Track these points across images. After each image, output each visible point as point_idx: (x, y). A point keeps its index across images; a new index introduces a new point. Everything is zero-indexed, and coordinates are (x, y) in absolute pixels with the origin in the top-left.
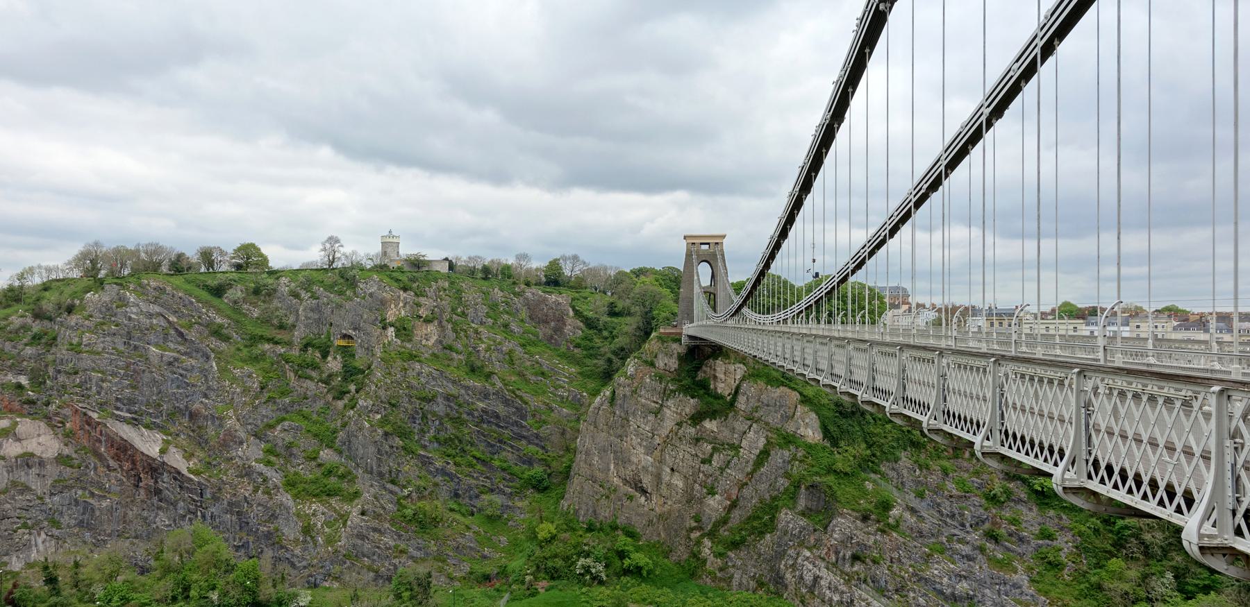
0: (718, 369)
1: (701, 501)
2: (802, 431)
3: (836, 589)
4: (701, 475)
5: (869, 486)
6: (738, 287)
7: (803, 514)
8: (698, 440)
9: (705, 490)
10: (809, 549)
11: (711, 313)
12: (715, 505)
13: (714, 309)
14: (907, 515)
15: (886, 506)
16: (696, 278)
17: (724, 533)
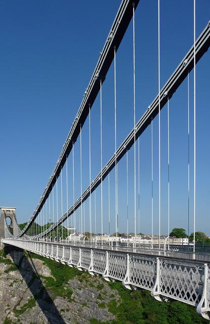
0: (14, 254)
1: (9, 300)
2: (44, 273)
3: (56, 321)
4: (9, 291)
5: (65, 288)
6: (21, 227)
7: (44, 299)
8: (8, 279)
9: (11, 296)
10: (47, 310)
11: (11, 236)
12: (15, 300)
13: (12, 233)
14: (76, 296)
15: (71, 293)
16: (5, 223)
17: (18, 308)
